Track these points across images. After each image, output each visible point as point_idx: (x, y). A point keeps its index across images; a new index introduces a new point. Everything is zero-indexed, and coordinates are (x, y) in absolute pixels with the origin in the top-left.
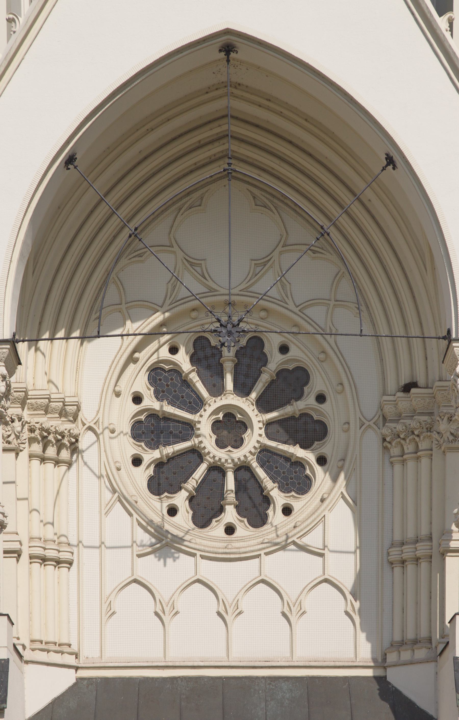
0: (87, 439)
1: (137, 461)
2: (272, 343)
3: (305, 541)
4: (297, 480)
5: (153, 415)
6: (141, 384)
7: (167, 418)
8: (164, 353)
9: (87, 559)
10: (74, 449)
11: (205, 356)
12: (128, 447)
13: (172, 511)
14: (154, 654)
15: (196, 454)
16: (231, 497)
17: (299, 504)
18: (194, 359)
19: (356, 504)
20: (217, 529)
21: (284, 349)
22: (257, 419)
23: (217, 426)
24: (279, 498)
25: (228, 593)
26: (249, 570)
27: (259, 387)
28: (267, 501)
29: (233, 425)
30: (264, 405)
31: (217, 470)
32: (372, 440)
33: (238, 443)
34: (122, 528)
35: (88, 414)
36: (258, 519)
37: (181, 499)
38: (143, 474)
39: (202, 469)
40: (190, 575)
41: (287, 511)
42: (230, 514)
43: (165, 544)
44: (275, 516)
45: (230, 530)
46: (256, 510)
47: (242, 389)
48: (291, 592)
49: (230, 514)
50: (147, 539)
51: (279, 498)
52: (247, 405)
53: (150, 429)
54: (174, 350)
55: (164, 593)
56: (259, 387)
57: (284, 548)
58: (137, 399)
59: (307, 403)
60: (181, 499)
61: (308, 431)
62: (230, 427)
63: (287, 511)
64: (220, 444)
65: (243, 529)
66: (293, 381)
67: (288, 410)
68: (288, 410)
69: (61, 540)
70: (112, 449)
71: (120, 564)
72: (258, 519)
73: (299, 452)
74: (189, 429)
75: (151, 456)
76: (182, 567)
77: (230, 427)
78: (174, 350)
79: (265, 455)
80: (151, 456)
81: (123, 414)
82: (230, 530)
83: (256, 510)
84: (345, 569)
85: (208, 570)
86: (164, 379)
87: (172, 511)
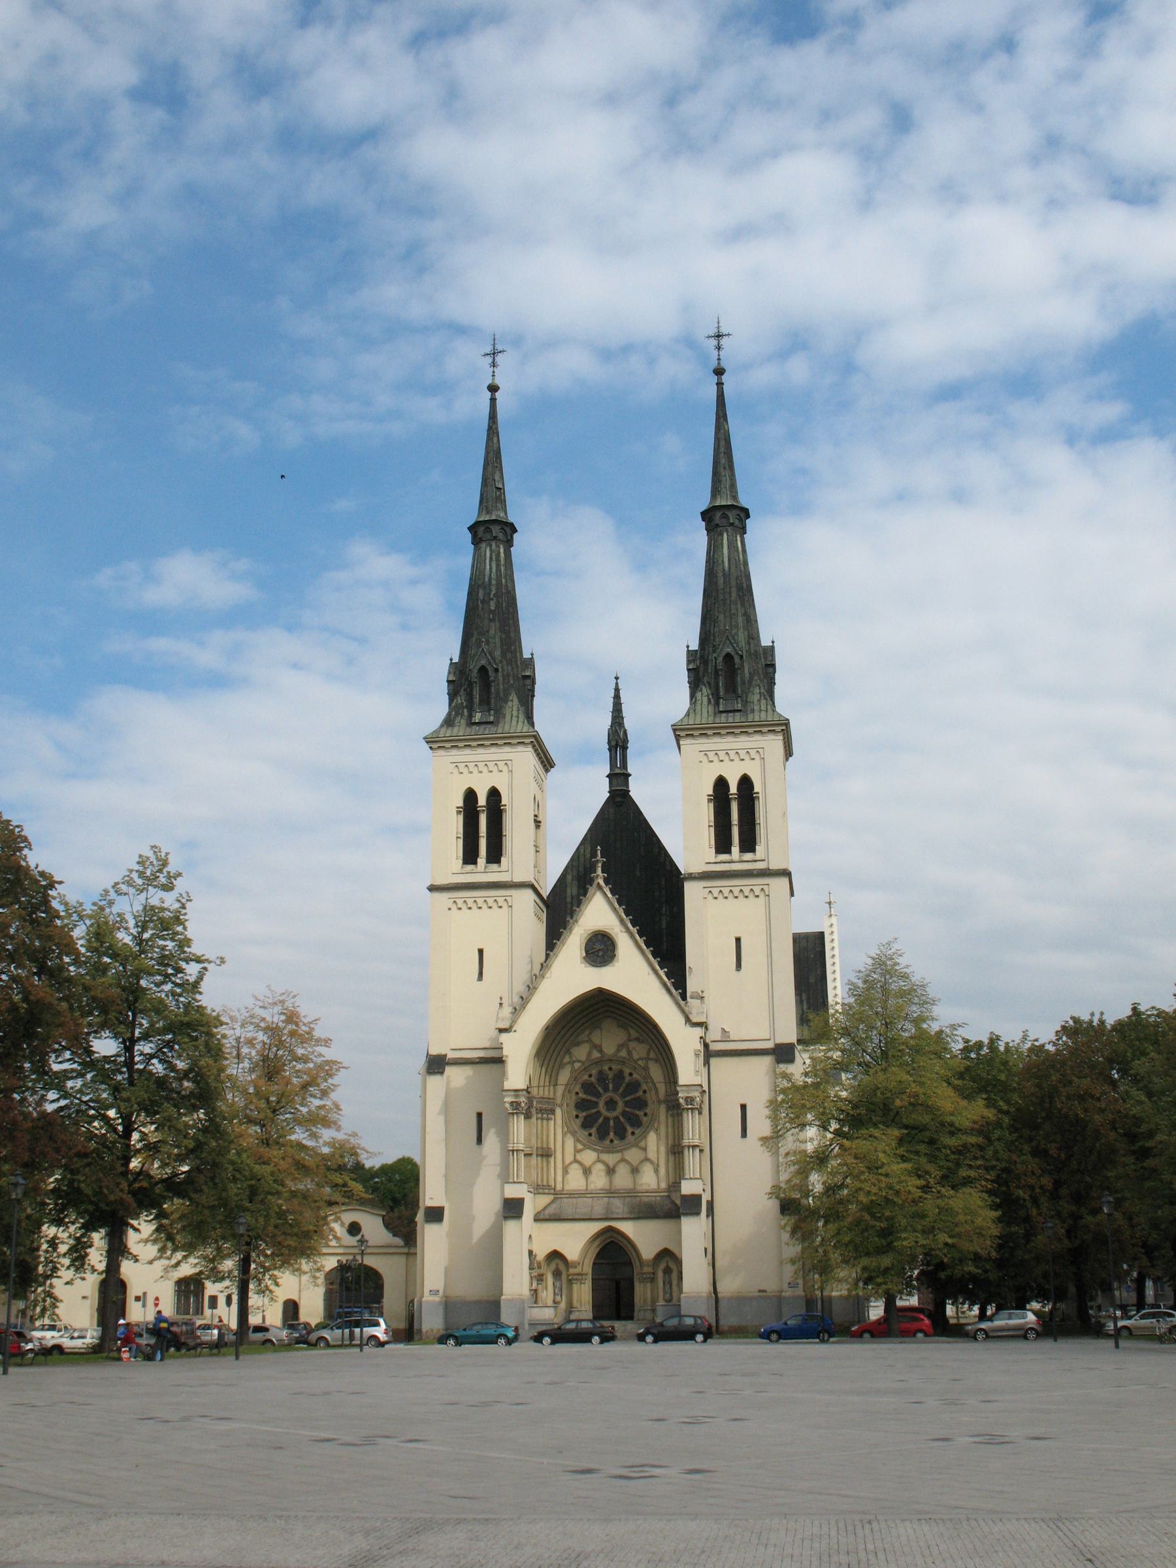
7: (588, 1100)
21: (631, 1074)
23: (607, 1103)
31: (607, 1119)
32: (663, 1108)
39: (601, 1119)
41: (633, 1133)
45: (612, 1141)
62: (611, 1104)
64: (608, 1110)
77: (611, 1104)
86: (587, 1087)
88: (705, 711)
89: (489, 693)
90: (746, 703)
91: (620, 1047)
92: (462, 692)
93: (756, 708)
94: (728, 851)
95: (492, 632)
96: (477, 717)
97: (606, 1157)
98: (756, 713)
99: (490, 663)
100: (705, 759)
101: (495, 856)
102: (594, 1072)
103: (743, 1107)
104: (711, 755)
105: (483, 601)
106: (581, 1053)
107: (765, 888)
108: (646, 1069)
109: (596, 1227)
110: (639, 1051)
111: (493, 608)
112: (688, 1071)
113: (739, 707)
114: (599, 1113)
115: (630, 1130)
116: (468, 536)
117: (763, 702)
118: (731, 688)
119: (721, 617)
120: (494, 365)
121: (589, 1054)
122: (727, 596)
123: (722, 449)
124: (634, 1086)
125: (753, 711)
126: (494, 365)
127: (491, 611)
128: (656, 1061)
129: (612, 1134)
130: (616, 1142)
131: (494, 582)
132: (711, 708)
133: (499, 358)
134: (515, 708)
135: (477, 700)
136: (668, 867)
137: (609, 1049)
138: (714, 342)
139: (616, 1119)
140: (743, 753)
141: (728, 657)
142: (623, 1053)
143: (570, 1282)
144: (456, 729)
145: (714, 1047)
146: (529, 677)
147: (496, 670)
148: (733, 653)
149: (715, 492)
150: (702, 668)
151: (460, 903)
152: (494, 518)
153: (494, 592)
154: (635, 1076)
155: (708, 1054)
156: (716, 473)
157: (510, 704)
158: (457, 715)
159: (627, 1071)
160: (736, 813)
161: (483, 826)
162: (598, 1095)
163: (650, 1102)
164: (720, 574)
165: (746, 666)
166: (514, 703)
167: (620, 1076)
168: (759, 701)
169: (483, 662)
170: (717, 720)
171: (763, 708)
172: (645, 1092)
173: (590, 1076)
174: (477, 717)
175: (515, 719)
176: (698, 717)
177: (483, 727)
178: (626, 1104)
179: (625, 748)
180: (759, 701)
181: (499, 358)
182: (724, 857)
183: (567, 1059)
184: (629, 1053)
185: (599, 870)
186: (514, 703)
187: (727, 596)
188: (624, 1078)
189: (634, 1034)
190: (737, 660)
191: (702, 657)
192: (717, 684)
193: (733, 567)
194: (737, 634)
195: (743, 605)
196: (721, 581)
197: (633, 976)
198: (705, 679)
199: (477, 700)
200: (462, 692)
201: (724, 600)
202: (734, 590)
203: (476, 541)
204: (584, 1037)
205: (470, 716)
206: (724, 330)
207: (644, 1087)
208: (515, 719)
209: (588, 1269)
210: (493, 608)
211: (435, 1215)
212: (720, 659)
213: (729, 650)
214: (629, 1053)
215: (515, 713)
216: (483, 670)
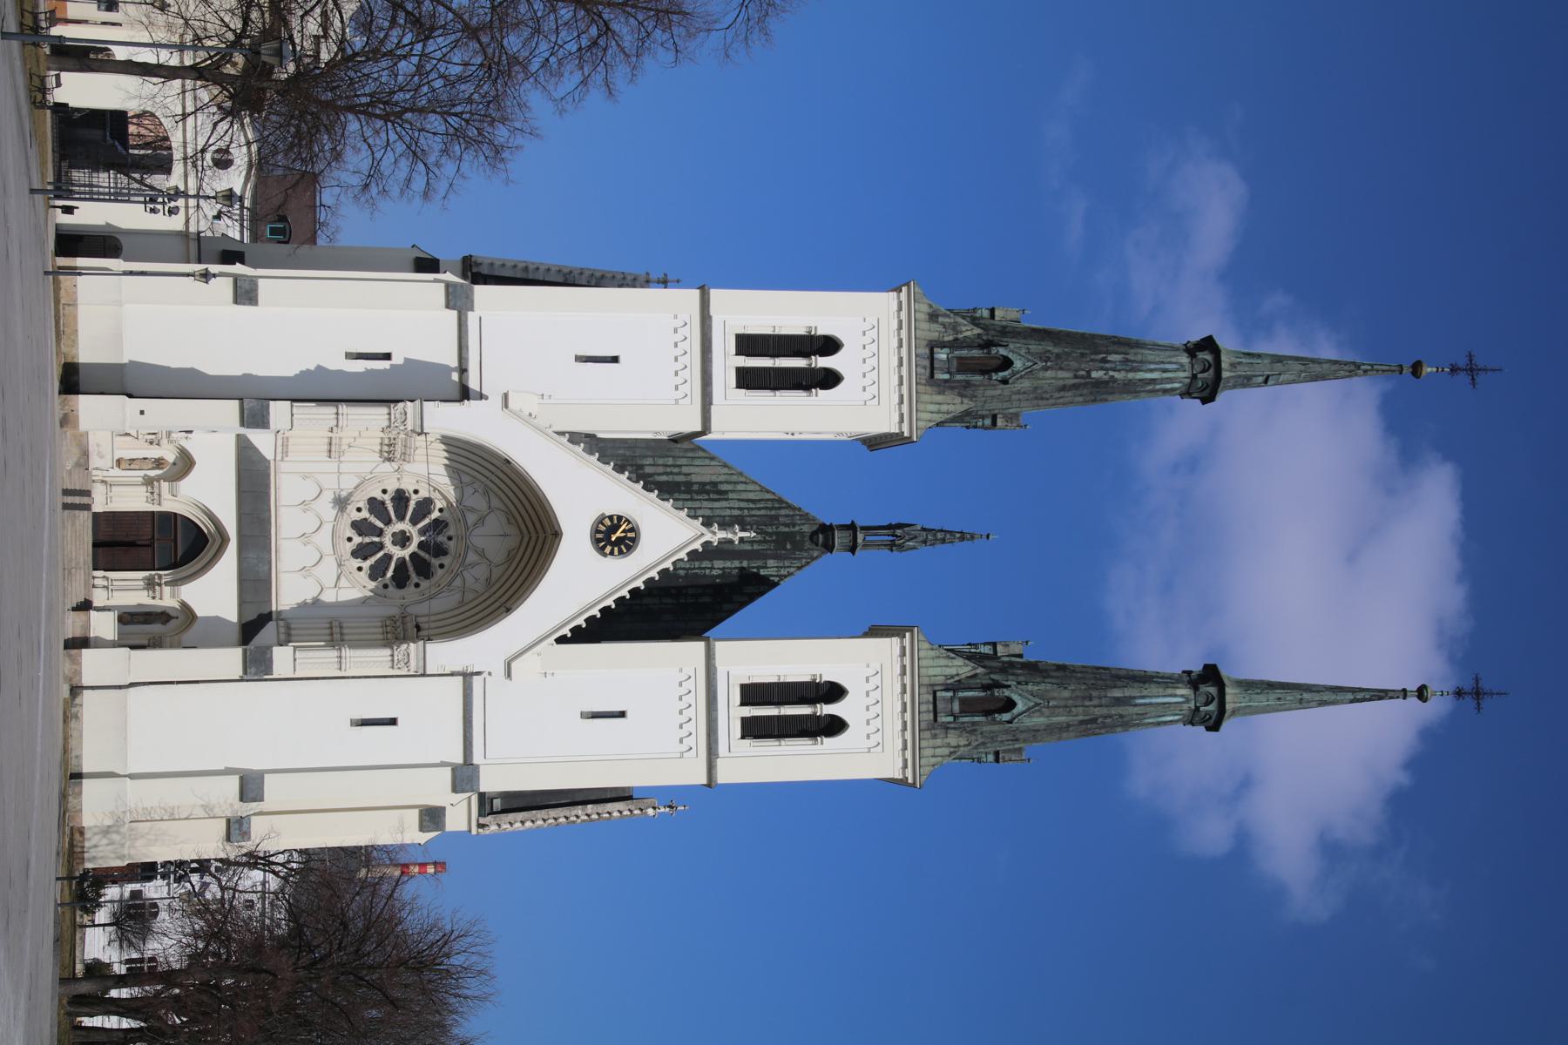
0: (395, 465)
1: (384, 491)
2: (446, 560)
3: (343, 579)
4: (376, 572)
5: (408, 500)
6: (424, 494)
7: (407, 507)
8: (439, 505)
9: (333, 466)
10: (389, 460)
11: (438, 525)
12: (392, 487)
13: (359, 510)
14: (283, 501)
15: (388, 522)
16: (367, 540)
17: (364, 575)
18: (436, 520)
19: (364, 601)
20: (350, 533)
21: (442, 566)
22: (405, 554)
23: (403, 532)
24: (366, 565)
25: (316, 538)
26: (328, 549)
27: (422, 554)
28: (365, 559)
29: (402, 540)
30: (413, 555)
31: (380, 533)
32: (395, 611)
33: (394, 543)
34: (348, 484)
35: (407, 467)
36: (355, 554)
37: (365, 514)
38: (378, 495)
39: (379, 524)
40: (325, 518)
41: (360, 569)
42: (357, 540)
43: (341, 503)
44: (357, 563)
45: (350, 539)
46: (361, 552)
47: (421, 545)
48: (316, 571)
49: (357, 540)
50: (344, 494)
51: (366, 565)
53: (401, 498)
54: (441, 510)
55: (314, 505)
56: (422, 554)
57: (340, 565)
58: (416, 492)
59: (414, 578)
60: (365, 514)
61: (401, 579)
62: (402, 539)
63: (360, 569)
64: (394, 534)
65: (350, 547)
66: (423, 569)
67: (411, 569)
68: (411, 569)
69: (341, 453)
70: (386, 480)
71: (332, 486)
72: (355, 554)
73: (390, 574)
74: (401, 518)
75: (387, 498)
76: (329, 512)
77: (402, 539)
78: (441, 510)
79: (388, 557)
80: (387, 498)
81: (408, 485)
82: (350, 539)
83: (361, 552)
84: (329, 597)
85: (327, 528)
86: (425, 506)
87: (359, 510)
88: (938, 671)
89: (973, 371)
90: (946, 728)
91: (482, 554)
92: (977, 331)
93: (939, 742)
94: (744, 702)
95: (1061, 374)
96: (942, 355)
98: (932, 742)
99: (1014, 374)
100: (871, 671)
101: (748, 380)
103: (393, 722)
104: (875, 681)
105: (1104, 361)
107: (693, 752)
110: (476, 575)
111: (1094, 374)
112: (445, 654)
113: (943, 719)
116: (1196, 337)
117: (946, 751)
118: (968, 707)
119: (1066, 694)
121: (472, 510)
122: (1095, 702)
123: (1306, 696)
125: (935, 737)
127: (1089, 372)
128: (462, 603)
131: (1131, 375)
132: (940, 680)
134: (951, 408)
135: (964, 353)
136: (726, 607)
137: (478, 539)
138: (1468, 685)
140: (877, 723)
141: (1010, 704)
143: (149, 482)
144: (925, 325)
145: (477, 681)
146: (994, 423)
147: (1005, 381)
148: (1015, 711)
149: (1248, 686)
150: (995, 664)
151: (685, 331)
152: (1225, 374)
153: (1116, 375)
154: (440, 572)
155: (467, 676)
156: (1271, 686)
157: (958, 400)
158: (944, 325)
162: (414, 522)
164: (1128, 692)
165: (996, 728)
166: (954, 404)
167: (440, 551)
168: (948, 746)
169: (1018, 364)
170: (924, 690)
171: (938, 751)
172: (417, 585)
174: (942, 355)
175: (934, 408)
176: (931, 663)
177: (927, 363)
179: (891, 546)
180: (948, 746)
181: (1463, 378)
182: (736, 696)
184: (473, 565)
185: (722, 535)
186: (954, 404)
187: (1095, 702)
188: (436, 556)
189: (497, 573)
190: (1006, 717)
191: (1011, 664)
192: (970, 689)
193: (1136, 710)
194: (1042, 715)
195: (1082, 722)
196: (1117, 693)
197: (580, 580)
198: (980, 670)
199: (964, 353)
200: (977, 331)
201: (1090, 698)
202: (1105, 711)
203: (1192, 350)
204: (495, 502)
205: (943, 345)
206: (1487, 702)
207: (424, 584)
208: (934, 408)
209: (169, 505)
210: (1094, 374)
211: (245, 294)
212: (1007, 693)
213: (1020, 707)
214: (473, 565)
215: (944, 408)
216: (1007, 363)
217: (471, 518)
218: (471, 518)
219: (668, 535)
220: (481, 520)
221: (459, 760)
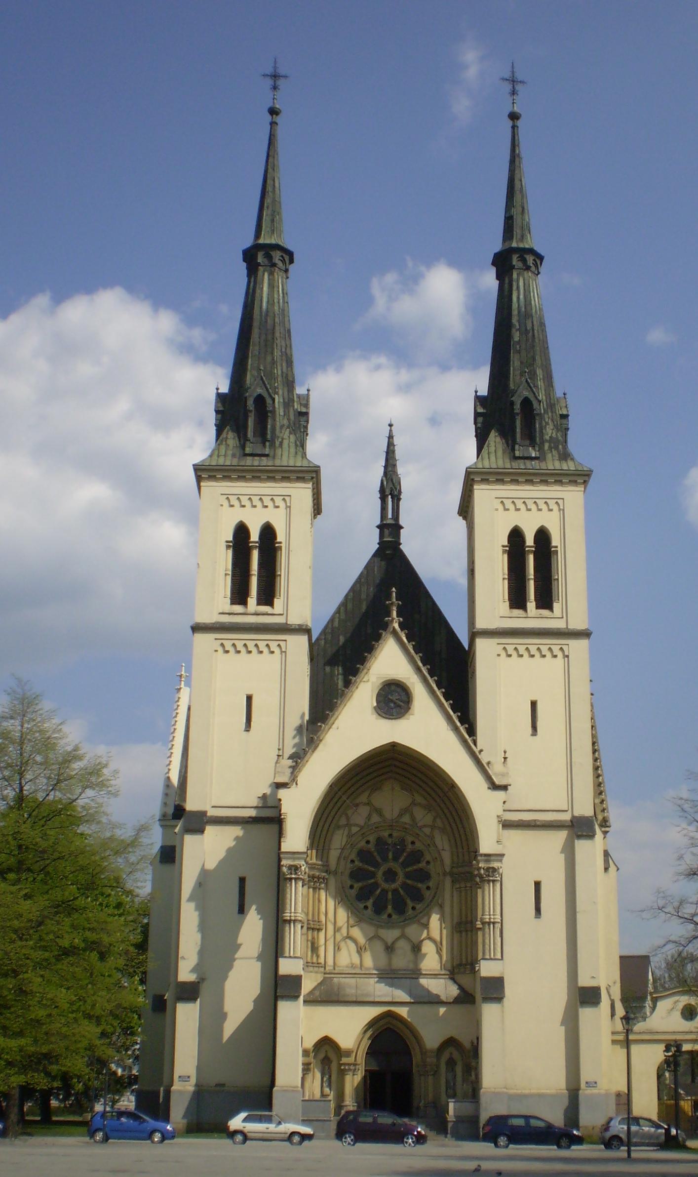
23: (384, 874)
24: (410, 904)
32: (448, 882)
45: (390, 916)
52: (396, 867)
83: (400, 908)
86: (363, 855)
91: (403, 812)
97: (383, 933)
102: (372, 838)
106: (360, 816)
108: (432, 837)
109: (374, 1012)
110: (423, 817)
114: (376, 885)
115: (410, 904)
120: (275, 88)
121: (369, 817)
124: (416, 856)
126: (275, 88)
129: (390, 907)
130: (394, 917)
133: (281, 82)
139: (395, 891)
142: (406, 819)
159: (409, 839)
160: (532, 567)
161: (255, 562)
163: (433, 874)
172: (428, 863)
173: (368, 842)
178: (407, 876)
183: (343, 821)
184: (413, 818)
204: (363, 798)
217: (375, 819)
218: (375, 819)
219: (391, 660)
220: (379, 812)
221: (563, 835)
